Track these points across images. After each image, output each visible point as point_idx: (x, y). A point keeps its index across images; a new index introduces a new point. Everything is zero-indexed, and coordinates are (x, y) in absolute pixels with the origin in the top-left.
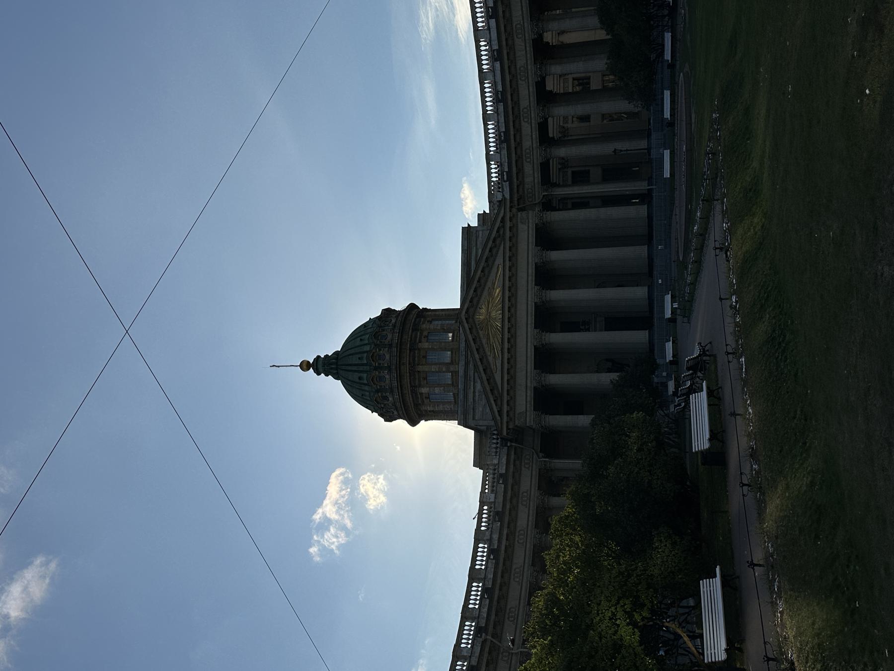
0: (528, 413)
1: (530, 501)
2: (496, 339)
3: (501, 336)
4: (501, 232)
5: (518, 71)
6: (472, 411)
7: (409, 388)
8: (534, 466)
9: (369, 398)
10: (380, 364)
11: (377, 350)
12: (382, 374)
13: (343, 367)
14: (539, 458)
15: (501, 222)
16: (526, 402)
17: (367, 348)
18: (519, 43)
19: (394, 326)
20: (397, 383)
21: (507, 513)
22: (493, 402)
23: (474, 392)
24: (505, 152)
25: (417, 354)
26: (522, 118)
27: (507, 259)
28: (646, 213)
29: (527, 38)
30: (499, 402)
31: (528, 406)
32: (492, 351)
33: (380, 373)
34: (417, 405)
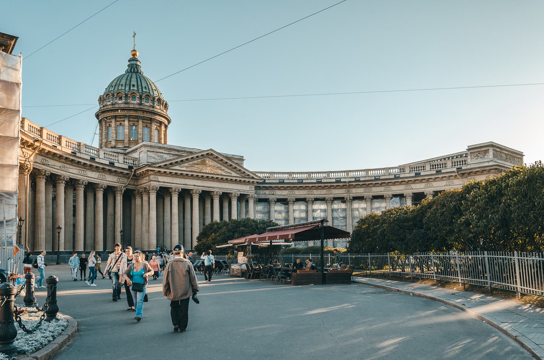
1: (101, 180)
2: (196, 168)
5: (311, 190)
8: (119, 184)
9: (120, 88)
10: (143, 99)
12: (137, 99)
14: (123, 187)
17: (152, 93)
18: (324, 191)
23: (162, 153)
24: (275, 181)
26: (290, 191)
30: (165, 167)
32: (190, 166)
33: (138, 98)
34: (115, 117)
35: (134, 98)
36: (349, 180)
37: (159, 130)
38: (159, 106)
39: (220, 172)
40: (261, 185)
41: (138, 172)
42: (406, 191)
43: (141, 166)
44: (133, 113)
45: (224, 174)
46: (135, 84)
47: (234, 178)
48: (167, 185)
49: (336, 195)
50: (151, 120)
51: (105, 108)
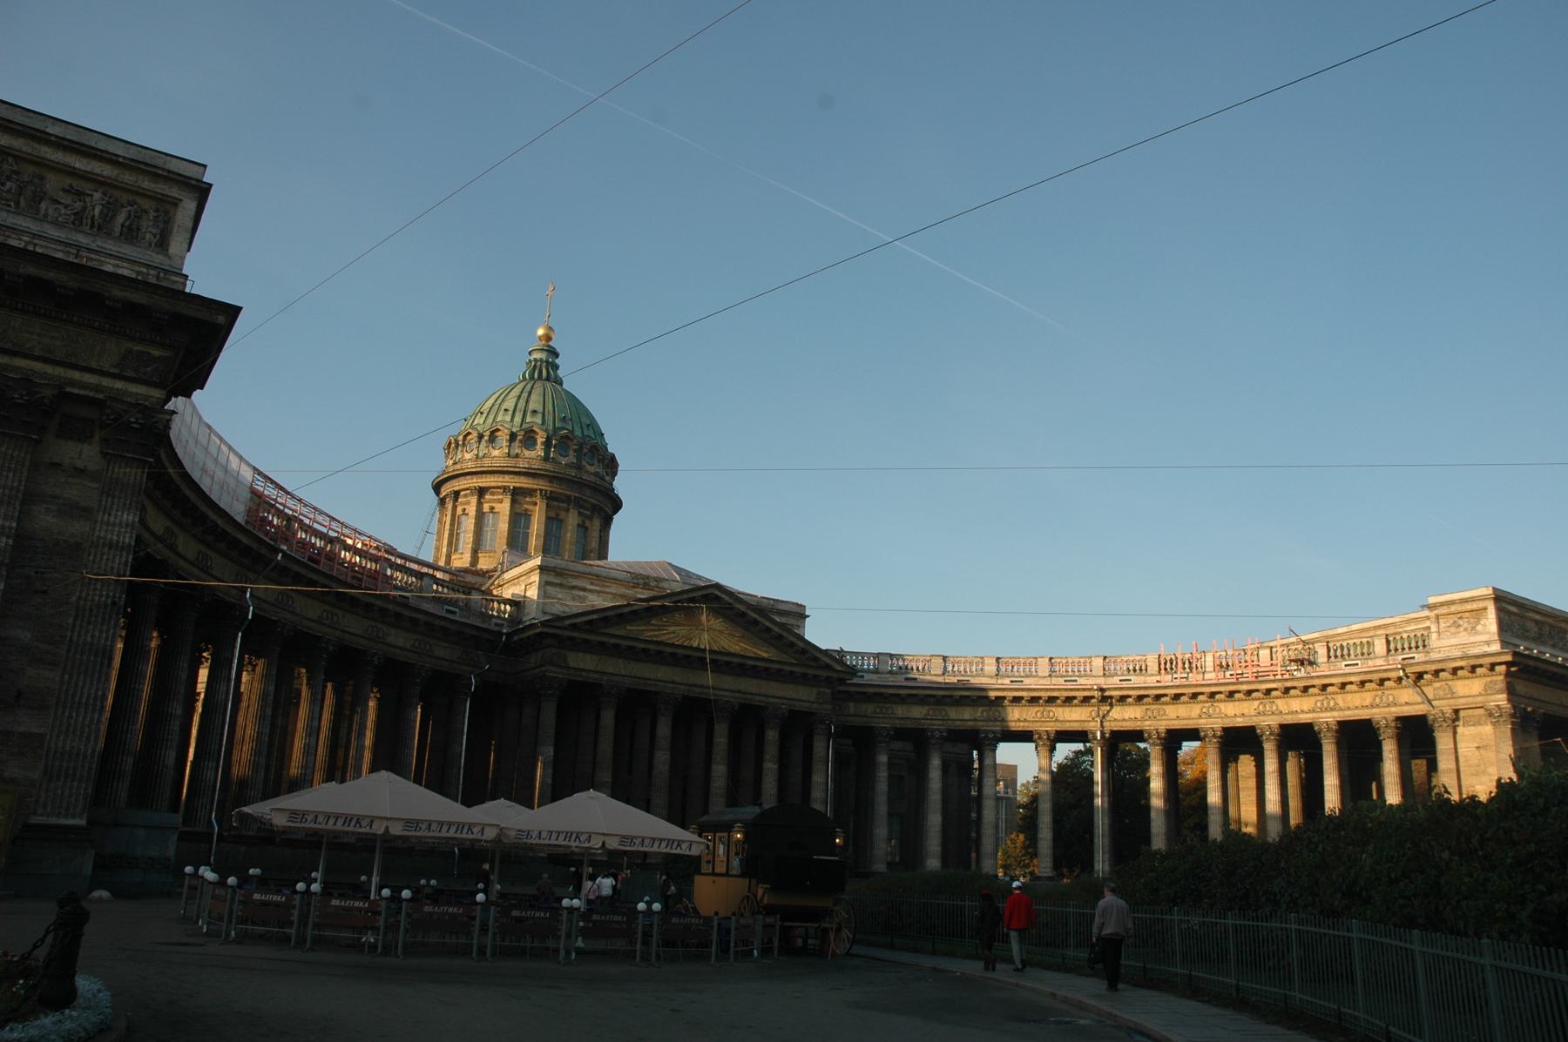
0: (565, 671)
3: (676, 643)
6: (559, 581)
7: (514, 484)
11: (575, 447)
12: (539, 446)
16: (582, 670)
17: (578, 433)
19: (602, 479)
20: (525, 468)
22: (590, 618)
23: (584, 590)
25: (562, 505)
27: (780, 667)
34: (481, 492)
37: (587, 528)
38: (592, 465)
41: (516, 638)
43: (528, 623)
46: (540, 409)
51: (458, 466)
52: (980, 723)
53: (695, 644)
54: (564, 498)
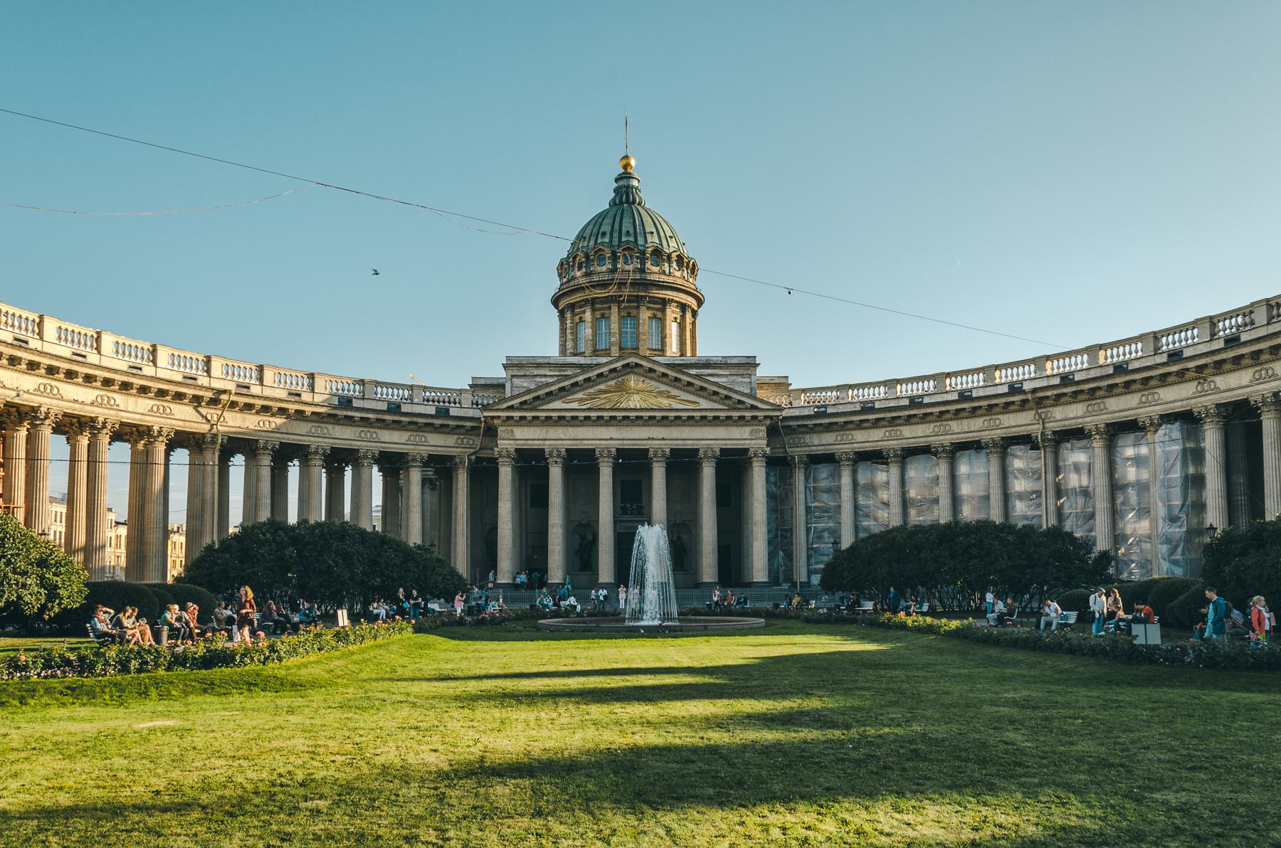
0: (512, 442)
2: (604, 401)
4: (740, 406)
5: (945, 423)
8: (459, 450)
12: (607, 261)
13: (619, 212)
15: (752, 406)
16: (526, 440)
17: (641, 241)
18: (977, 423)
21: (396, 418)
23: (546, 376)
24: (849, 408)
27: (703, 414)
28: (759, 580)
29: (983, 433)
31: (522, 442)
33: (609, 258)
34: (572, 307)
35: (601, 259)
36: (1044, 383)
37: (660, 319)
39: (665, 402)
40: (808, 422)
42: (1199, 400)
44: (600, 293)
45: (675, 405)
47: (697, 414)
48: (533, 445)
49: (1009, 430)
50: (638, 300)
52: (932, 438)
53: (623, 405)
54: (633, 298)
